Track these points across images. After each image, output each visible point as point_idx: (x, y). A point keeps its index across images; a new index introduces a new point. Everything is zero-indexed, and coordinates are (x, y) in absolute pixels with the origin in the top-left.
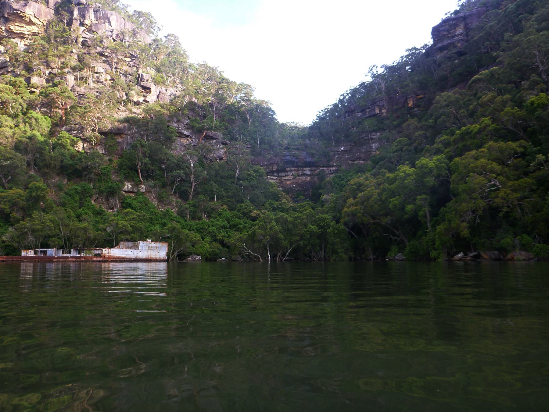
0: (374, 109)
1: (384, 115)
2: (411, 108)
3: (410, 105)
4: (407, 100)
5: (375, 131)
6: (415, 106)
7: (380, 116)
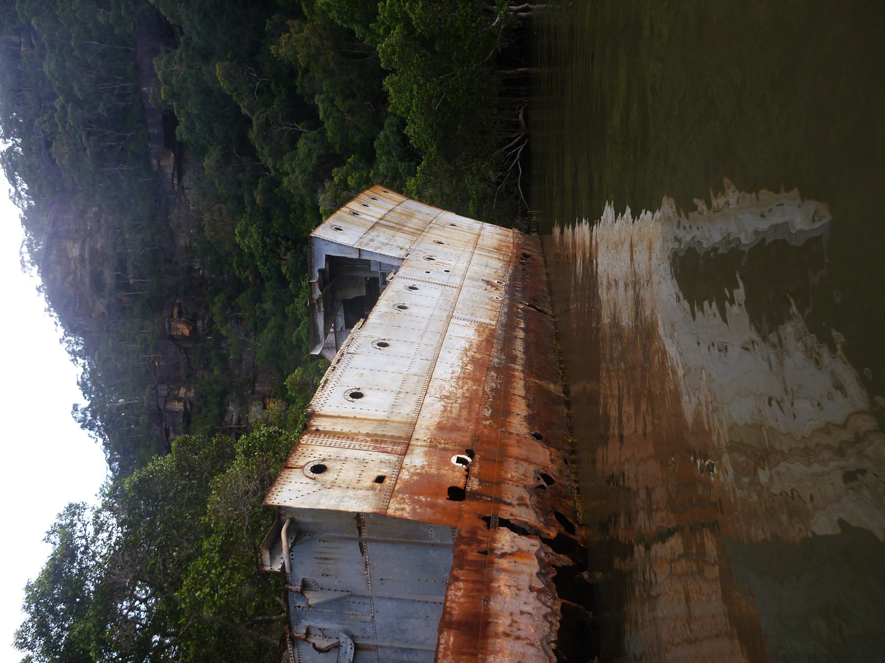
0: (174, 413)
1: (191, 394)
2: (194, 331)
3: (187, 332)
4: (172, 338)
5: (223, 413)
6: (192, 321)
7: (191, 403)
